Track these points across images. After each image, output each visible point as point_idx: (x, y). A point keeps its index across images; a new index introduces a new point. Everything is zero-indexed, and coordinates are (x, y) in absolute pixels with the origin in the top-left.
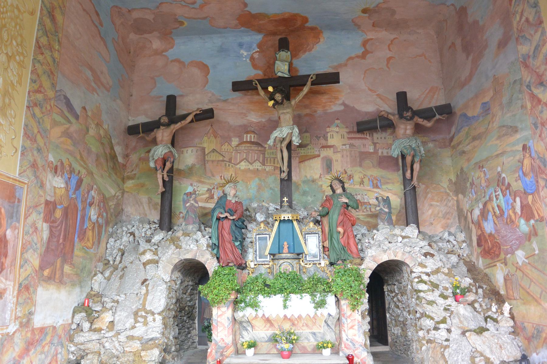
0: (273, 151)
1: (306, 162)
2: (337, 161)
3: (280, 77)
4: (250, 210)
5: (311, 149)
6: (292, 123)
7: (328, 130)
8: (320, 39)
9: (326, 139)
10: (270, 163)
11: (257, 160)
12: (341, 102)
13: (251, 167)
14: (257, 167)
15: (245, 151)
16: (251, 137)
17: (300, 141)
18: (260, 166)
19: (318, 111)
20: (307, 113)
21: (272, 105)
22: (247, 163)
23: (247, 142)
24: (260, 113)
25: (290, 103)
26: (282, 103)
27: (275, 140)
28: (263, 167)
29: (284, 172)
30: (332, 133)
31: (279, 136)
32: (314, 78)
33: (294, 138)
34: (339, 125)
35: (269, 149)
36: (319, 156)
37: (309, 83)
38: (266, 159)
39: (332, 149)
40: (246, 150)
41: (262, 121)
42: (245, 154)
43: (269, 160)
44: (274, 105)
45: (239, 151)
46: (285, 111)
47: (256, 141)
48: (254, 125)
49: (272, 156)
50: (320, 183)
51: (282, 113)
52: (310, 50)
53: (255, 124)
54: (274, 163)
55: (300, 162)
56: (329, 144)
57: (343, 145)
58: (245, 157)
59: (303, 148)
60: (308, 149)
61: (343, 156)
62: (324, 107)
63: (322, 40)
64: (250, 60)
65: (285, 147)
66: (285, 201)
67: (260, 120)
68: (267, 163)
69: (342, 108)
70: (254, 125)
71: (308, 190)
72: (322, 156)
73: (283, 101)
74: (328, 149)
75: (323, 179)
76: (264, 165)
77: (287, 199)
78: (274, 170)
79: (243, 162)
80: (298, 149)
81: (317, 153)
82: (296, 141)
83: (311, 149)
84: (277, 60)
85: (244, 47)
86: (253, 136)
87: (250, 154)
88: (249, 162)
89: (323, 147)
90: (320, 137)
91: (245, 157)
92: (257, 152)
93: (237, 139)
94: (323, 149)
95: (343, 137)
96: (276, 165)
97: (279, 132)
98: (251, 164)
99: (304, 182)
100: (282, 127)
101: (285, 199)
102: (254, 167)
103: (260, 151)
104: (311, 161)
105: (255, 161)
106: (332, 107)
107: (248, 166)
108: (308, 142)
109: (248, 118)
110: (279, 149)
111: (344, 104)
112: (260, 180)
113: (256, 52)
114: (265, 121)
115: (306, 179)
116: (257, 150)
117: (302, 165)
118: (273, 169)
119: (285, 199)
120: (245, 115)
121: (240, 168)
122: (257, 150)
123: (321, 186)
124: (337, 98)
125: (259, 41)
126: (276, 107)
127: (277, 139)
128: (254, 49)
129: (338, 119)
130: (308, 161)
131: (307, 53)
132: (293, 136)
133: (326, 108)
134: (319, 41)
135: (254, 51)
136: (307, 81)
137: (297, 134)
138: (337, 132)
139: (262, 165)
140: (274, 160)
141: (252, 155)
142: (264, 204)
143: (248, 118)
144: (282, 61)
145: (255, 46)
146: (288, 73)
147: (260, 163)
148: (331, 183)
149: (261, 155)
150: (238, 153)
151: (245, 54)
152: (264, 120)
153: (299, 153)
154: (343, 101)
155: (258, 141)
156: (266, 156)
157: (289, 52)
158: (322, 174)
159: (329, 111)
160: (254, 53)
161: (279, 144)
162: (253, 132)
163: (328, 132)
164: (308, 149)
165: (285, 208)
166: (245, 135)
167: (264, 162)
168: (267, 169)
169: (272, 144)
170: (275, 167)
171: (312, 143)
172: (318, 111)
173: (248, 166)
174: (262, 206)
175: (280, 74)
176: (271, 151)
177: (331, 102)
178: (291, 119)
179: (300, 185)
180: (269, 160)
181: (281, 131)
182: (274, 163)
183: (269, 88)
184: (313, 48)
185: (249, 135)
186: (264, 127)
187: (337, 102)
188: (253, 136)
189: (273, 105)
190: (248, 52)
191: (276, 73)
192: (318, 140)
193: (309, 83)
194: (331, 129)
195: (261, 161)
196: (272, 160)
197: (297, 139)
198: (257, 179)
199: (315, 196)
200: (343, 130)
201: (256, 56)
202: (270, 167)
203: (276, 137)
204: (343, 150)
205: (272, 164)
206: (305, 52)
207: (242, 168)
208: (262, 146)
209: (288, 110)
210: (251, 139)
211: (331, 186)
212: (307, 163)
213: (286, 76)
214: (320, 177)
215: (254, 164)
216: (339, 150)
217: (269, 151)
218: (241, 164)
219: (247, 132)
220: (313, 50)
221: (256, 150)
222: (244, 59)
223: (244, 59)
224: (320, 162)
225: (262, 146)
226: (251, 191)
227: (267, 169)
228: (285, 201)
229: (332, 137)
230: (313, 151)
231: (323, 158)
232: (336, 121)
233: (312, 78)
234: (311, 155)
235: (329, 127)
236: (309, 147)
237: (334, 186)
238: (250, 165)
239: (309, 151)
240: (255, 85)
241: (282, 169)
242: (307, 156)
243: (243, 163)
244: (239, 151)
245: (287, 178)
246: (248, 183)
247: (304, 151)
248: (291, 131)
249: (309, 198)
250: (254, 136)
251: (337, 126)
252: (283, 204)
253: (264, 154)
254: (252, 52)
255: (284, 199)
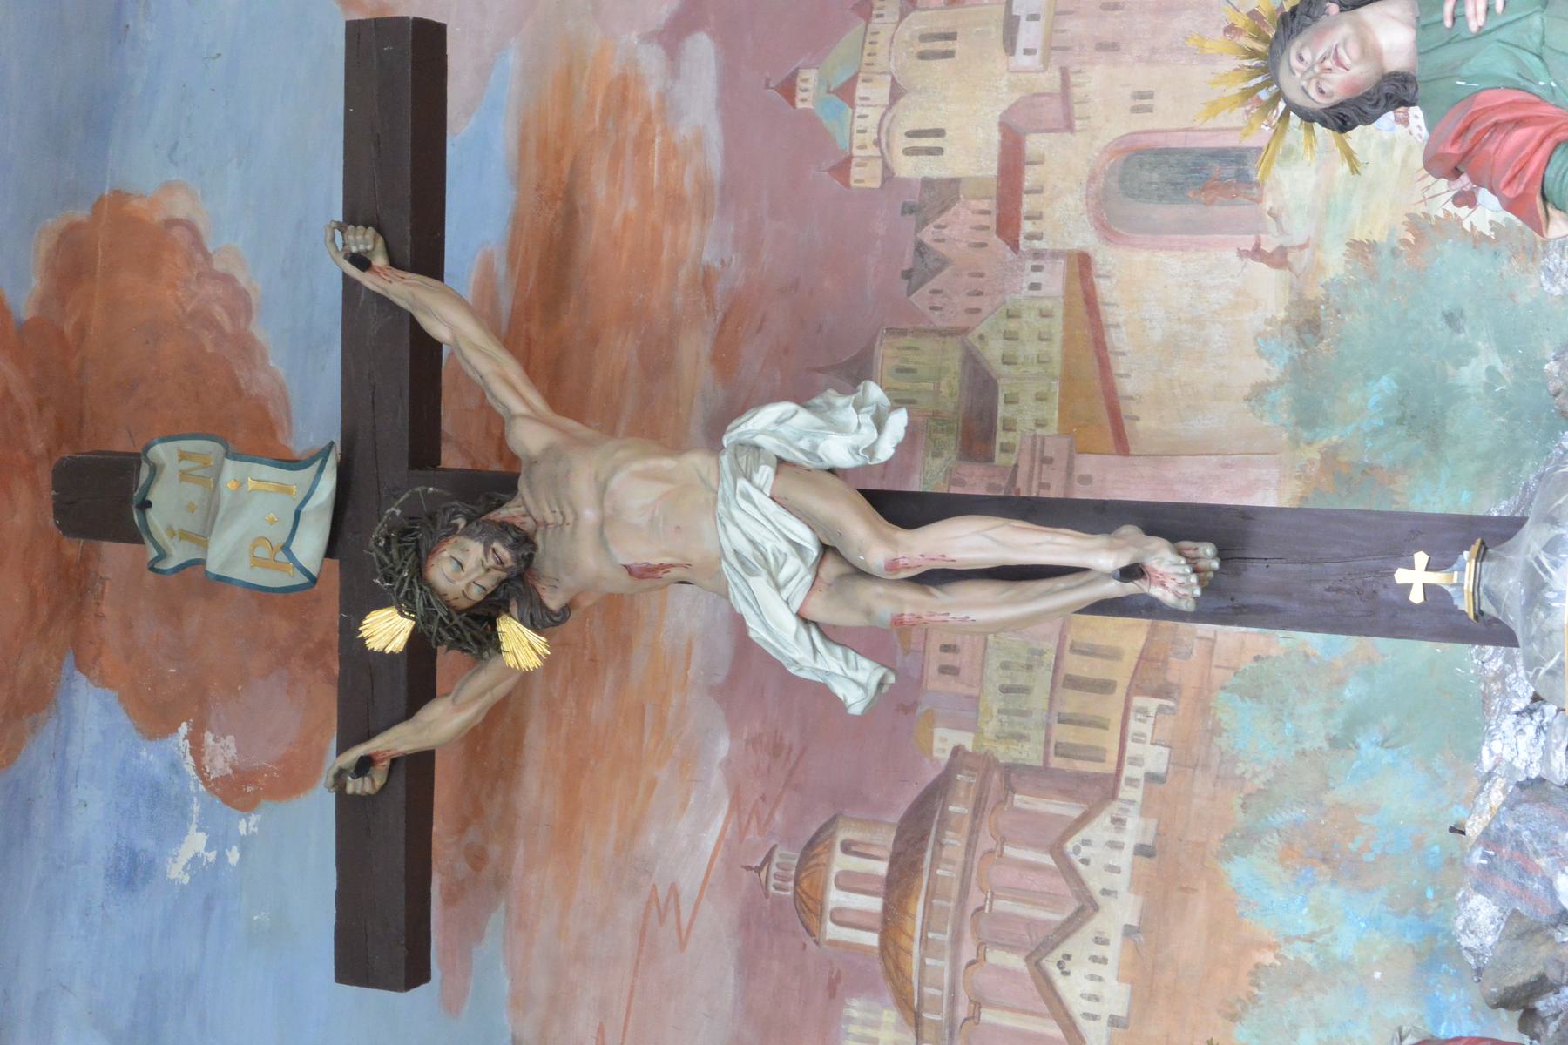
0: (992, 688)
1: (1127, 386)
2: (1142, 101)
3: (330, 552)
4: (1520, 975)
5: (1010, 337)
6: (696, 461)
7: (865, 176)
8: (171, 223)
9: (943, 193)
10: (1101, 725)
11: (1057, 851)
12: (651, 60)
13: (1121, 911)
14: (1124, 859)
15: (968, 952)
16: (850, 882)
17: (875, 392)
18: (1118, 822)
19: (709, 256)
20: (706, 348)
21: (539, 642)
22: (1079, 945)
23: (891, 923)
24: (663, 775)
25: (533, 462)
26: (523, 542)
27: (830, 634)
28: (1126, 792)
29: (1132, 572)
30: (900, 142)
31: (798, 590)
32: (363, 240)
33: (838, 451)
34: (841, 78)
35: (973, 727)
36: (1083, 263)
37: (404, 289)
38: (1056, 762)
39: (1035, 144)
40: (957, 939)
41: (728, 763)
42: (995, 957)
43: (1066, 734)
44: (539, 620)
45: (962, 1012)
46: (589, 515)
47: (885, 839)
48: (752, 836)
49: (1038, 700)
50: (1335, 261)
51: (603, 543)
52: (241, 303)
53: (742, 831)
54: (1105, 687)
55: (1122, 444)
56: (991, 169)
57: (1010, 44)
58: (1016, 962)
59: (1002, 411)
60: (1008, 361)
61: (1109, 47)
62: (675, 202)
63: (181, 208)
64: (247, 806)
65: (902, 535)
66: (1436, 578)
67: (717, 780)
68: (1097, 755)
69: (702, 49)
70: (752, 836)
71: (1386, 385)
72: (1084, 238)
73: (505, 528)
74: (1030, 177)
75: (1299, 229)
76: (1107, 788)
77: (1421, 558)
78: (1163, 692)
79: (1061, 983)
80: (1000, 458)
81: (1053, 281)
82: (868, 433)
83: (1010, 337)
84: (200, 563)
85: (146, 844)
86: (841, 862)
87: (1002, 905)
88: (1067, 929)
89: (1008, 223)
90: (921, 249)
91: (1016, 962)
92: (986, 842)
93: (856, 1008)
94: (1027, 227)
95: (939, 47)
96: (1121, 674)
97: (760, 585)
98: (1087, 907)
99: (1308, 415)
100: (723, 555)
101: (1415, 577)
102: (1121, 882)
103: (978, 811)
104: (1118, 339)
105: (1067, 870)
106: (684, 131)
107: (1101, 941)
108: (953, 359)
109: (689, 880)
110: (914, 603)
111: (672, 36)
112: (1246, 840)
113: (197, 750)
114: (734, 734)
115: (1280, 396)
116: (974, 832)
117: (1145, 424)
118: (1152, 704)
119: (1415, 577)
120: (662, 906)
121: (1114, 1021)
122: (974, 832)
123: (1361, 250)
124: (623, 93)
125: (122, 718)
126: (554, 602)
127: (818, 612)
128: (175, 767)
129: (788, 90)
130: (1120, 366)
131: (262, 331)
132: (812, 453)
133: (688, 186)
134: (190, 226)
135: (189, 765)
136: (383, 301)
137: (804, 418)
138: (896, 94)
139: (1113, 809)
140: (1075, 683)
141: (1017, 894)
142: (1474, 828)
143: (689, 880)
144: (210, 515)
145: (151, 757)
146: (308, 474)
147: (1084, 819)
148: (1308, 117)
149: (1020, 800)
150: (974, 1017)
151: (196, 842)
152: (723, 747)
153: (1037, 444)
154: (647, 38)
155: (895, 818)
156: (1029, 753)
157: (162, 452)
158: (1248, 243)
159: (715, 161)
160: (199, 768)
161: (868, 594)
162: (813, 850)
163: (888, 175)
164: (1008, 361)
165: (1511, 586)
166: (832, 931)
167: (1082, 778)
168: (1155, 758)
169: (868, 672)
170: (1137, 686)
171: (961, 321)
172: (706, 257)
173: (1101, 941)
174: (1490, 839)
175: (310, 545)
176: (993, 701)
177: (642, 145)
178: (667, 463)
179: (1330, 455)
180: (1066, 734)
181: (760, 563)
182: (1105, 687)
183: (375, 644)
184: (227, 279)
185: (836, 898)
186: (776, 749)
187: (652, 91)
188: (841, 862)
189: (534, 625)
190: (185, 817)
191: (301, 579)
192: (943, 263)
193: (404, 289)
194: (862, 147)
195: (1073, 811)
196: (1073, 702)
197: (849, 416)
198: (1238, 871)
199: (1452, 319)
200: (883, 39)
201: (223, 753)
202: (1134, 726)
203: (804, 620)
204: (1053, 47)
205: (1111, 707)
206: (246, 347)
207: (1116, 997)
208: (940, 789)
209: (582, 486)
210: (868, 877)
211: (1342, 118)
212: (1131, 382)
213: (327, 484)
214: (1279, 259)
215: (1095, 884)
216: (1049, 80)
217: (990, 727)
218: (1077, 1006)
219: (809, 907)
220: (242, 280)
221: (970, 846)
222: (234, 856)
223: (234, 856)
224: (1141, 257)
225: (940, 789)
226: (1345, 944)
227: (1155, 758)
228: (1436, 578)
229: (928, 139)
230: (1030, 317)
231: (1108, 230)
232: (806, 100)
233: (362, 262)
234: (1068, 341)
235: (842, 169)
236: (994, 350)
237: (1335, 87)
238: (1096, 924)
239: (1031, 349)
240: (378, 777)
241: (1114, 588)
242: (1069, 379)
243: (1073, 988)
244: (962, 1012)
245: (1208, 549)
246: (1268, 958)
247: (1027, 400)
248: (765, 473)
249: (1471, 375)
250: (847, 848)
251: (846, 92)
252: (1466, 605)
253: (1013, 775)
254: (196, 786)
255: (1417, 597)
